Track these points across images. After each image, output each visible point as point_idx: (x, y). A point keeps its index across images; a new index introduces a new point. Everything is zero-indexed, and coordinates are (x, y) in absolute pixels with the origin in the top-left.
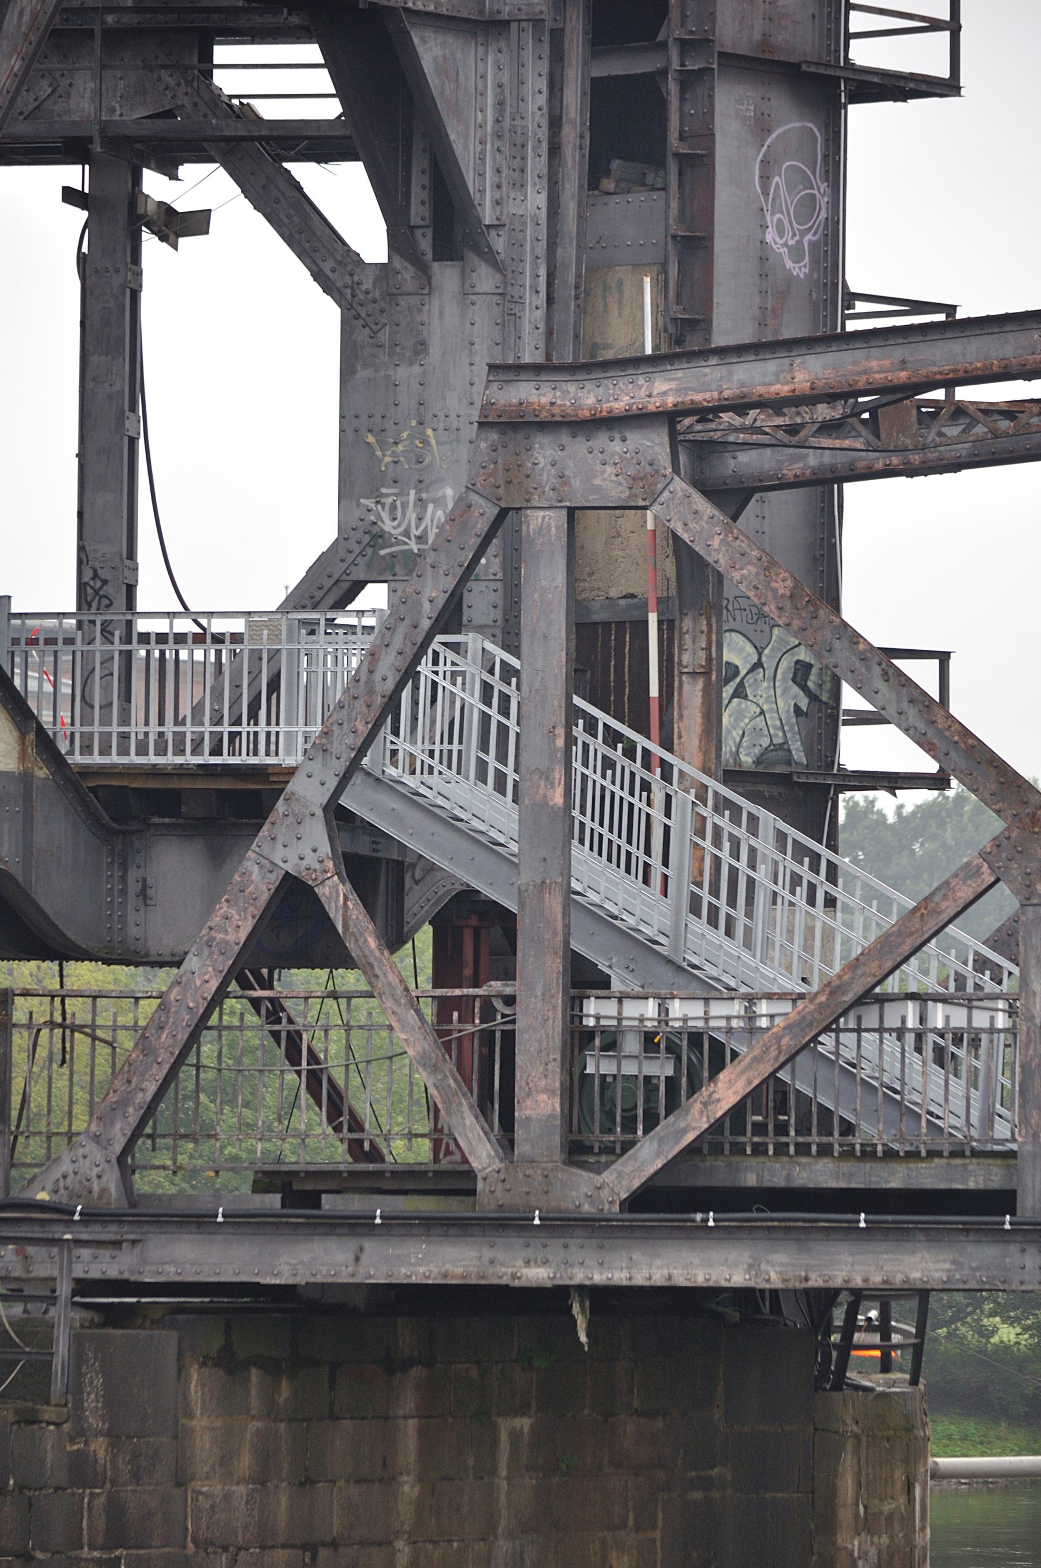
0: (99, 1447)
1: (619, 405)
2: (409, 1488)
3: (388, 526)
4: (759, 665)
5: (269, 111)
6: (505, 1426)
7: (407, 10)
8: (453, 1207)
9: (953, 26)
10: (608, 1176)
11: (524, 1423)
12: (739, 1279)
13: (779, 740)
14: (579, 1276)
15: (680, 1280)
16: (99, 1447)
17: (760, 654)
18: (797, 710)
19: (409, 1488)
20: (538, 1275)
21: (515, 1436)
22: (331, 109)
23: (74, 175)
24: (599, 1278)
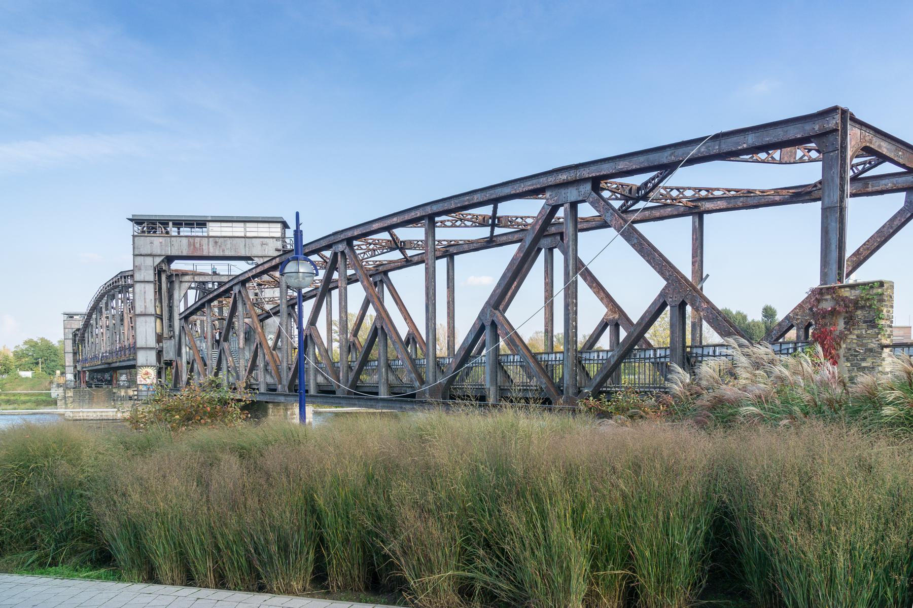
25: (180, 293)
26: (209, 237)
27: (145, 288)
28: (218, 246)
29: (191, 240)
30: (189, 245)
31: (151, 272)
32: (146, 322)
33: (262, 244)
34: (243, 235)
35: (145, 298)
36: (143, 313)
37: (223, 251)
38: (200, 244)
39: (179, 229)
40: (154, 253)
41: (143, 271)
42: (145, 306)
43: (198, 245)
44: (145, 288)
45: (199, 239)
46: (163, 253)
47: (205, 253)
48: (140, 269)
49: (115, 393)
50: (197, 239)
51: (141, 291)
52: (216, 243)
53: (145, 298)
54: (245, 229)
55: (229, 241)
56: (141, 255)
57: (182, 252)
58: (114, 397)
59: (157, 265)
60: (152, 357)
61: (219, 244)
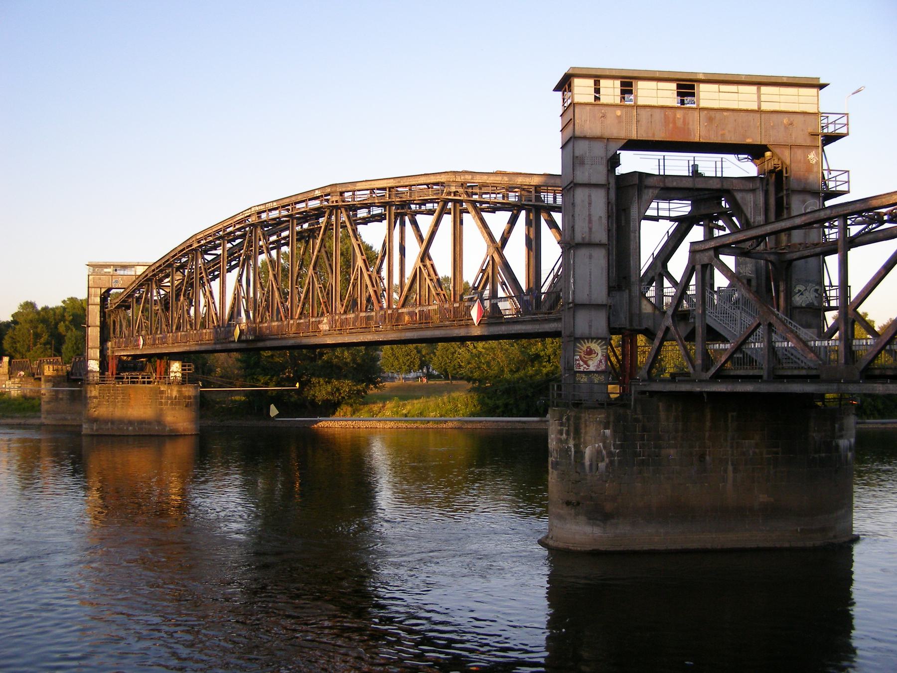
0: (640, 417)
2: (708, 424)
3: (741, 271)
4: (806, 289)
6: (730, 415)
7: (733, 189)
8: (688, 378)
10: (708, 373)
11: (735, 414)
13: (811, 301)
14: (703, 390)
15: (717, 390)
16: (640, 417)
17: (806, 288)
18: (816, 297)
19: (708, 424)
21: (732, 416)
24: (706, 390)
25: (639, 209)
27: (590, 196)
29: (669, 113)
31: (602, 169)
32: (590, 257)
35: (590, 215)
36: (587, 240)
40: (607, 134)
41: (587, 167)
42: (590, 229)
44: (590, 196)
48: (582, 163)
49: (162, 392)
51: (583, 201)
53: (590, 215)
58: (162, 398)
59: (611, 158)
60: (600, 322)
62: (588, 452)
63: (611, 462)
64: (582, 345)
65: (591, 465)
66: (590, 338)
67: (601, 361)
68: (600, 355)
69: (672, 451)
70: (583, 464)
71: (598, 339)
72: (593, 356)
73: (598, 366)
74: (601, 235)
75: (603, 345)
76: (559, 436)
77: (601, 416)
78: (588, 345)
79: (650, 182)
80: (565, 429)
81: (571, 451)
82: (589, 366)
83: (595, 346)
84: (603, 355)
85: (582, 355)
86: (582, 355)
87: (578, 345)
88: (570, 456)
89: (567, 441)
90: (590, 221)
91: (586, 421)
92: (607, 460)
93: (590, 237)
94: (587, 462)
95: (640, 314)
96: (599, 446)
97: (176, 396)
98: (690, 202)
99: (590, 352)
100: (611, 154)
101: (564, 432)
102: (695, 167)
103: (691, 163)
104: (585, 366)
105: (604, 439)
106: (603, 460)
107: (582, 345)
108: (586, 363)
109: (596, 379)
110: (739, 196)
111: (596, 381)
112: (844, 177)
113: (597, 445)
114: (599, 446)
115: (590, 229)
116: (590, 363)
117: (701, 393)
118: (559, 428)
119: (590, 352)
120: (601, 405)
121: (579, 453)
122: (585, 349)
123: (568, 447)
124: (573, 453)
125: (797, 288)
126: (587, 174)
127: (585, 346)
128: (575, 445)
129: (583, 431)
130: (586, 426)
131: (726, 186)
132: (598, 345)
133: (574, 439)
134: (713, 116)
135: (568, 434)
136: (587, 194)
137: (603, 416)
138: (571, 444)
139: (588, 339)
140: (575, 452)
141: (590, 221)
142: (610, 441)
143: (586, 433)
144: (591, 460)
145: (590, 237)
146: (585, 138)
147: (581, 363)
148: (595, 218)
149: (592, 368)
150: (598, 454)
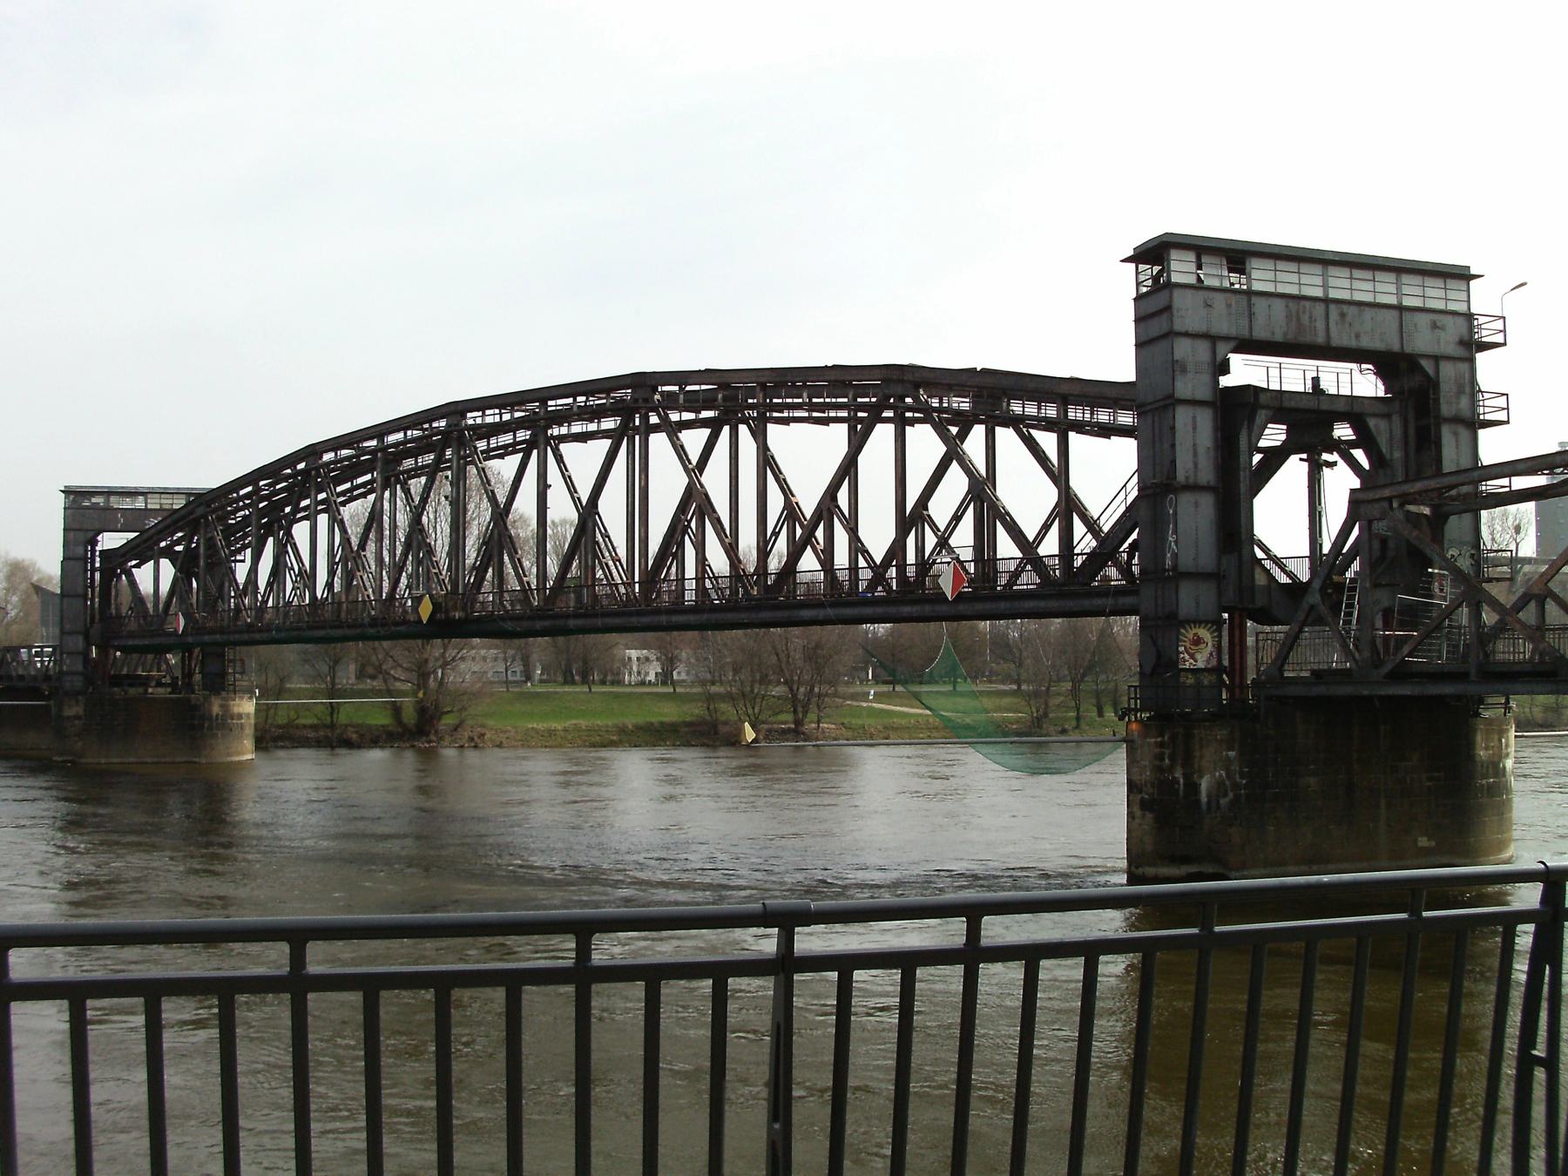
1: (1377, 497)
5: (1343, 438)
9: (1508, 409)
12: (1409, 693)
14: (1374, 693)
20: (1366, 693)
22: (1354, 437)
23: (1304, 456)
24: (1379, 693)
26: (1326, 301)
27: (1194, 418)
28: (1347, 326)
29: (1292, 305)
30: (1288, 317)
33: (1434, 326)
34: (1392, 300)
35: (1195, 445)
36: (1191, 480)
37: (1357, 336)
38: (1311, 317)
39: (1324, 276)
41: (1190, 375)
42: (1196, 464)
43: (1305, 319)
44: (1194, 418)
45: (1307, 304)
46: (1233, 332)
47: (1320, 339)
48: (1184, 370)
50: (1303, 303)
52: (1343, 315)
53: (1195, 445)
54: (1399, 288)
55: (1368, 314)
56: (1186, 334)
57: (1273, 333)
61: (1348, 319)
62: (1205, 784)
63: (1237, 798)
64: (1187, 631)
65: (1209, 802)
66: (1198, 622)
67: (1211, 654)
68: (1210, 644)
69: (1312, 780)
70: (1198, 801)
71: (1207, 622)
72: (1203, 646)
73: (1208, 661)
74: (1207, 475)
75: (1214, 632)
76: (1157, 763)
77: (1222, 733)
78: (1195, 631)
79: (1263, 398)
80: (1167, 752)
81: (1178, 783)
82: (1196, 661)
83: (1204, 633)
84: (1214, 646)
85: (1188, 645)
86: (1188, 645)
87: (1183, 631)
88: (1178, 790)
89: (1171, 769)
90: (1195, 454)
91: (1201, 739)
92: (1231, 795)
93: (1196, 476)
94: (1204, 798)
95: (1253, 587)
96: (1221, 775)
97: (217, 715)
98: (1285, 427)
99: (1198, 641)
100: (1219, 358)
101: (1166, 756)
102: (1316, 381)
103: (1311, 375)
104: (1191, 661)
105: (1227, 764)
106: (1225, 795)
107: (1187, 631)
108: (1192, 656)
109: (1206, 680)
110: (1372, 422)
111: (1206, 682)
112: (1502, 402)
113: (1217, 774)
114: (1221, 775)
115: (1196, 464)
116: (1198, 656)
117: (1369, 699)
118: (1157, 750)
119: (1198, 641)
120: (1219, 716)
121: (1193, 788)
122: (1191, 636)
123: (1174, 778)
124: (1182, 786)
125: (1450, 553)
126: (1190, 386)
127: (1190, 633)
128: (1185, 776)
129: (1197, 754)
130: (1201, 747)
131: (1357, 409)
132: (1211, 633)
133: (1183, 766)
134: (1345, 310)
135: (1172, 758)
136: (1191, 415)
137: (1225, 732)
138: (1179, 774)
139: (1195, 622)
140: (1184, 784)
141: (1195, 454)
142: (1235, 767)
143: (1201, 757)
144: (1209, 796)
145: (1196, 476)
146: (1186, 334)
147: (1187, 657)
148: (1201, 451)
149: (1201, 665)
150: (1219, 788)
